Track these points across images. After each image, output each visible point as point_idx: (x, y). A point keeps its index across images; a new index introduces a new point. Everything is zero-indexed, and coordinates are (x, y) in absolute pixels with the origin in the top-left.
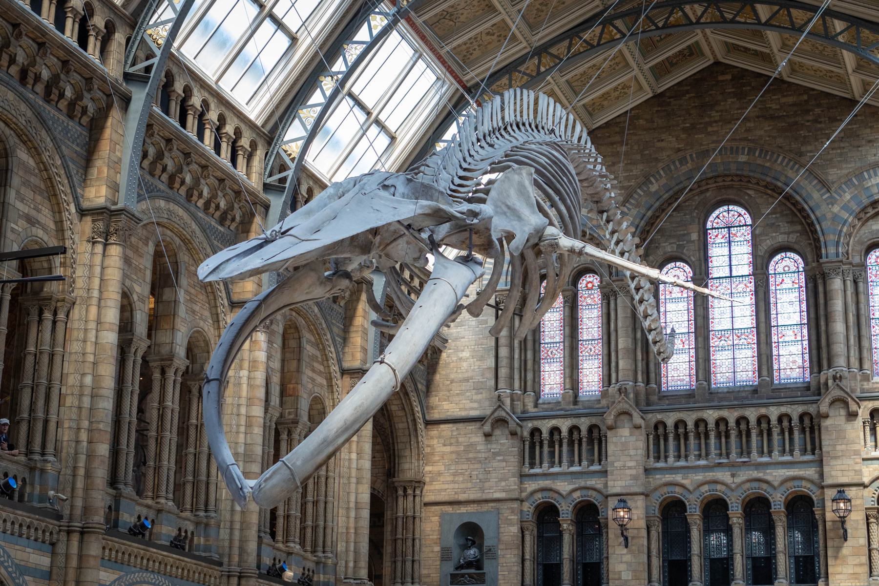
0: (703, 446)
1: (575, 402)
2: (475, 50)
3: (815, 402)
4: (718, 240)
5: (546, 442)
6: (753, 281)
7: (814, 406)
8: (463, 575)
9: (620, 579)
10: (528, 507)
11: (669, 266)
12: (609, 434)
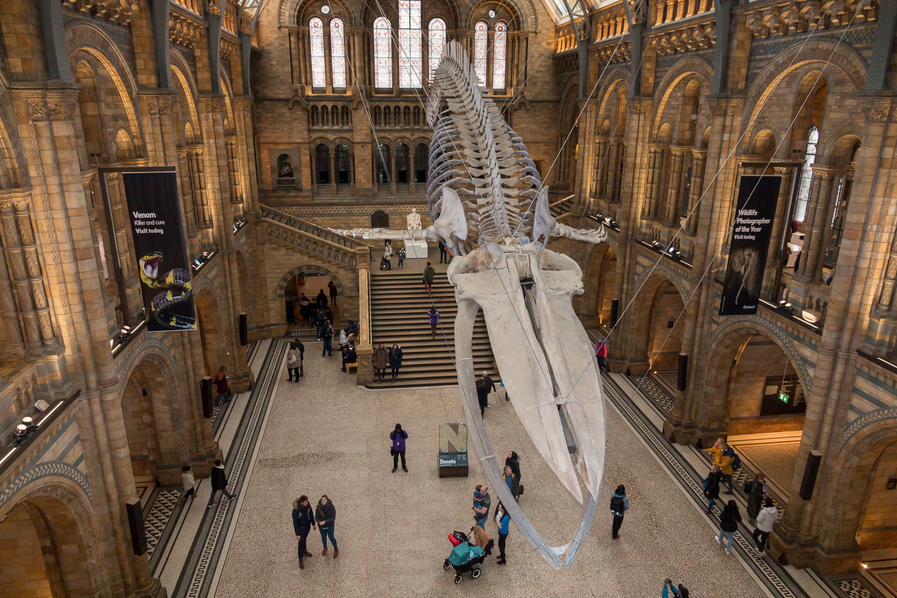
8: (283, 180)
10: (313, 146)
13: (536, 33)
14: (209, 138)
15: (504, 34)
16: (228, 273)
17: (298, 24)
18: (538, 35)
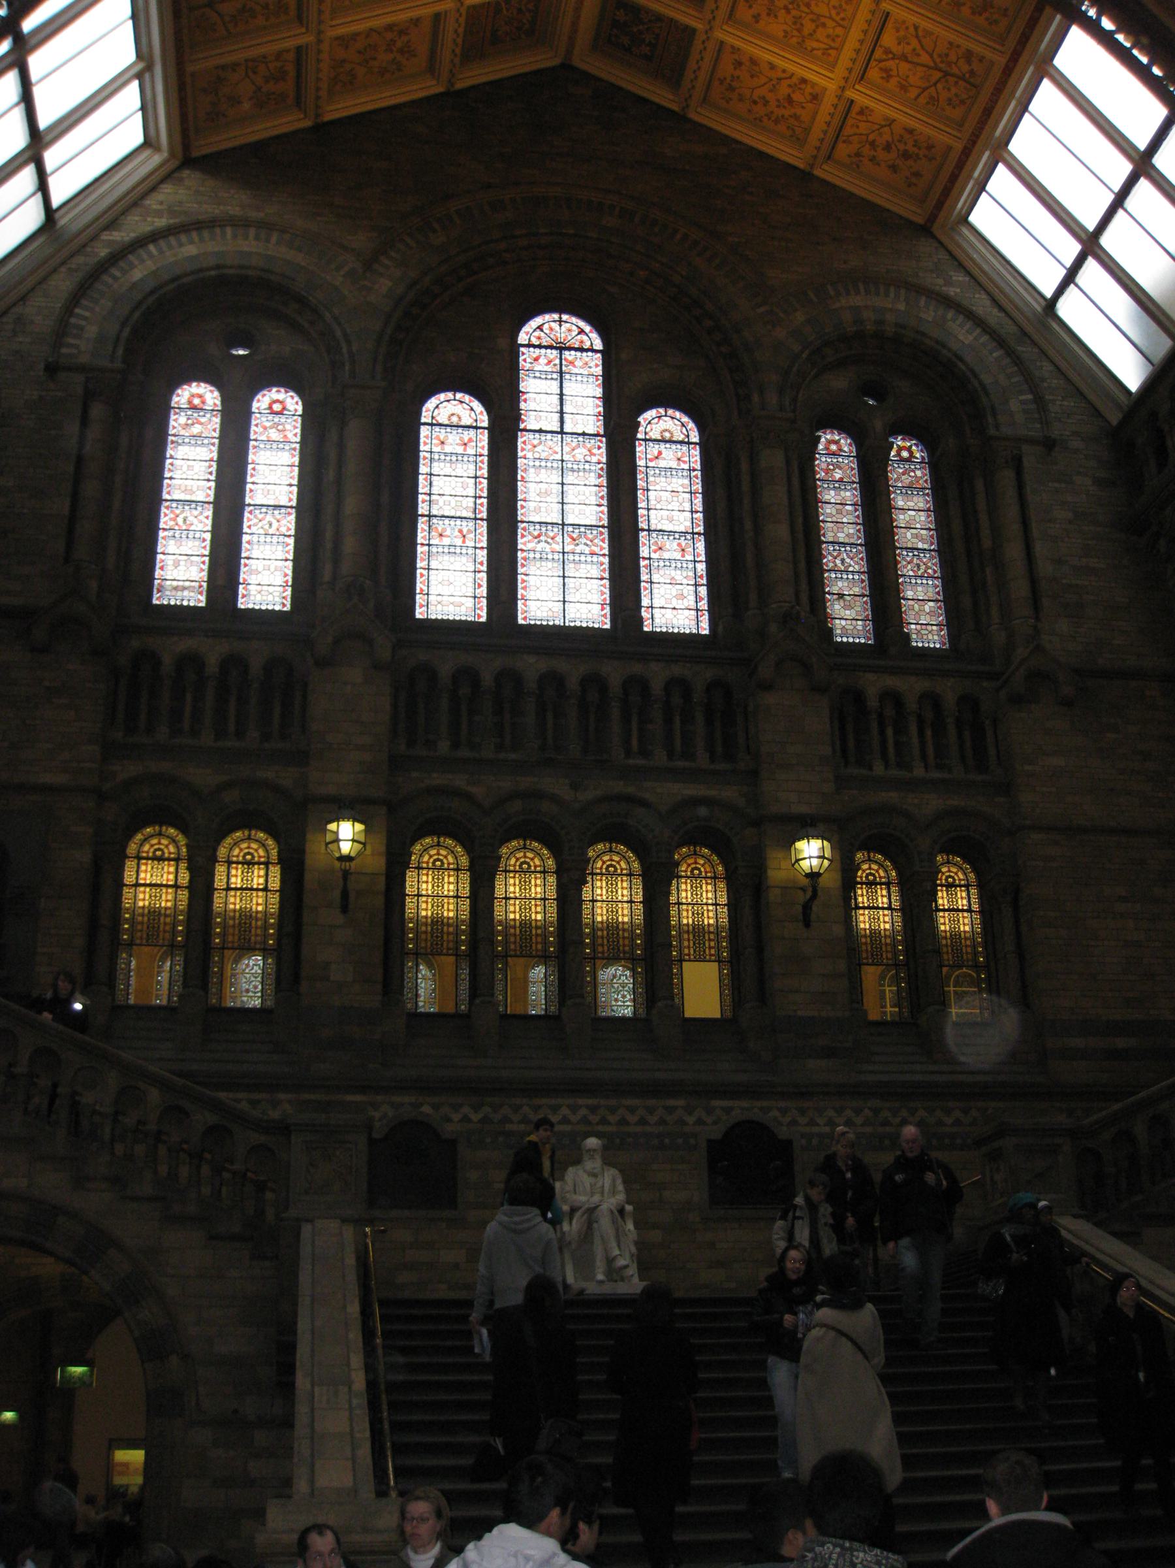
4: (541, 366)
6: (603, 445)
11: (442, 396)
15: (921, 474)
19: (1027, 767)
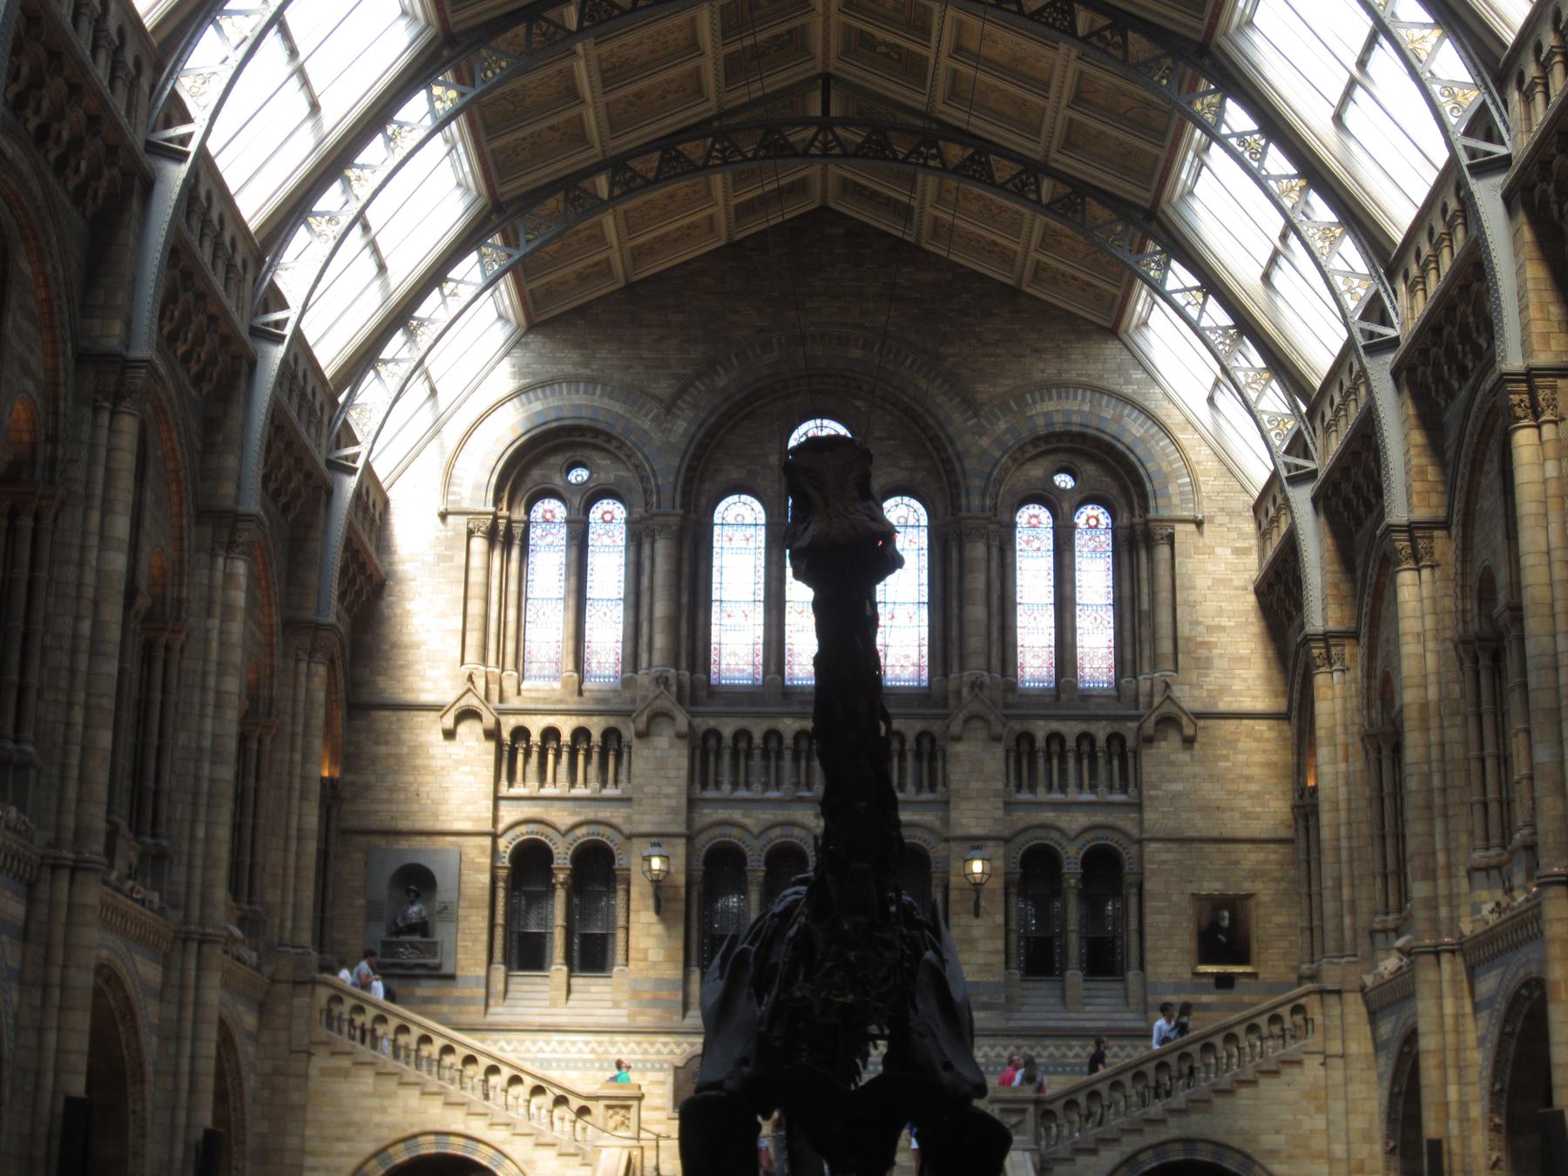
0: (773, 769)
1: (580, 693)
2: (524, 149)
3: (944, 717)
5: (535, 749)
7: (939, 722)
8: (402, 944)
9: (645, 959)
10: (506, 845)
12: (635, 743)
13: (1199, 524)
14: (209, 614)
15: (1106, 539)
16: (190, 996)
17: (497, 500)
18: (1206, 527)
19: (1152, 793)
